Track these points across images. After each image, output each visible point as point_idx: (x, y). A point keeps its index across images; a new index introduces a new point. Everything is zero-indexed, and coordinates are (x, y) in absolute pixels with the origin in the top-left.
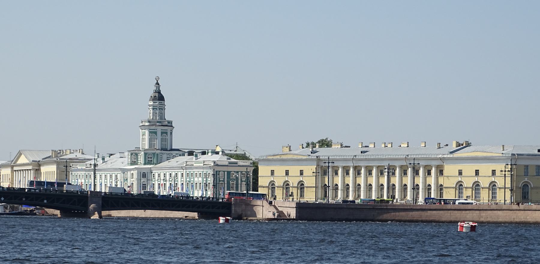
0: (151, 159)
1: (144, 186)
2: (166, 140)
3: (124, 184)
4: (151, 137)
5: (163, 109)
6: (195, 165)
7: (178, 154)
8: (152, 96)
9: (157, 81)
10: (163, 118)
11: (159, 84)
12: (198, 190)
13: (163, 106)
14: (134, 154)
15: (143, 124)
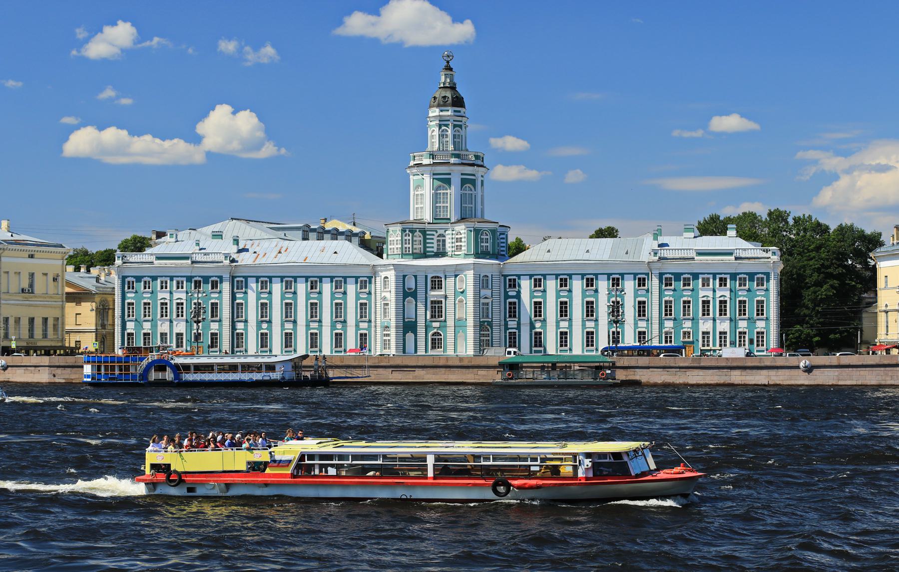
0: (487, 244)
1: (485, 307)
2: (472, 199)
3: (406, 303)
4: (466, 192)
5: (463, 128)
6: (696, 258)
7: (504, 234)
8: (437, 96)
9: (448, 62)
10: (463, 148)
11: (451, 69)
12: (714, 320)
13: (464, 119)
14: (418, 230)
15: (434, 161)
